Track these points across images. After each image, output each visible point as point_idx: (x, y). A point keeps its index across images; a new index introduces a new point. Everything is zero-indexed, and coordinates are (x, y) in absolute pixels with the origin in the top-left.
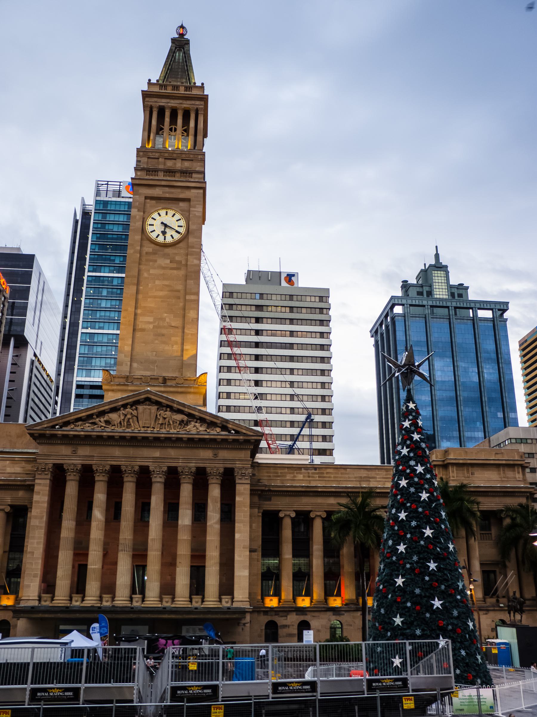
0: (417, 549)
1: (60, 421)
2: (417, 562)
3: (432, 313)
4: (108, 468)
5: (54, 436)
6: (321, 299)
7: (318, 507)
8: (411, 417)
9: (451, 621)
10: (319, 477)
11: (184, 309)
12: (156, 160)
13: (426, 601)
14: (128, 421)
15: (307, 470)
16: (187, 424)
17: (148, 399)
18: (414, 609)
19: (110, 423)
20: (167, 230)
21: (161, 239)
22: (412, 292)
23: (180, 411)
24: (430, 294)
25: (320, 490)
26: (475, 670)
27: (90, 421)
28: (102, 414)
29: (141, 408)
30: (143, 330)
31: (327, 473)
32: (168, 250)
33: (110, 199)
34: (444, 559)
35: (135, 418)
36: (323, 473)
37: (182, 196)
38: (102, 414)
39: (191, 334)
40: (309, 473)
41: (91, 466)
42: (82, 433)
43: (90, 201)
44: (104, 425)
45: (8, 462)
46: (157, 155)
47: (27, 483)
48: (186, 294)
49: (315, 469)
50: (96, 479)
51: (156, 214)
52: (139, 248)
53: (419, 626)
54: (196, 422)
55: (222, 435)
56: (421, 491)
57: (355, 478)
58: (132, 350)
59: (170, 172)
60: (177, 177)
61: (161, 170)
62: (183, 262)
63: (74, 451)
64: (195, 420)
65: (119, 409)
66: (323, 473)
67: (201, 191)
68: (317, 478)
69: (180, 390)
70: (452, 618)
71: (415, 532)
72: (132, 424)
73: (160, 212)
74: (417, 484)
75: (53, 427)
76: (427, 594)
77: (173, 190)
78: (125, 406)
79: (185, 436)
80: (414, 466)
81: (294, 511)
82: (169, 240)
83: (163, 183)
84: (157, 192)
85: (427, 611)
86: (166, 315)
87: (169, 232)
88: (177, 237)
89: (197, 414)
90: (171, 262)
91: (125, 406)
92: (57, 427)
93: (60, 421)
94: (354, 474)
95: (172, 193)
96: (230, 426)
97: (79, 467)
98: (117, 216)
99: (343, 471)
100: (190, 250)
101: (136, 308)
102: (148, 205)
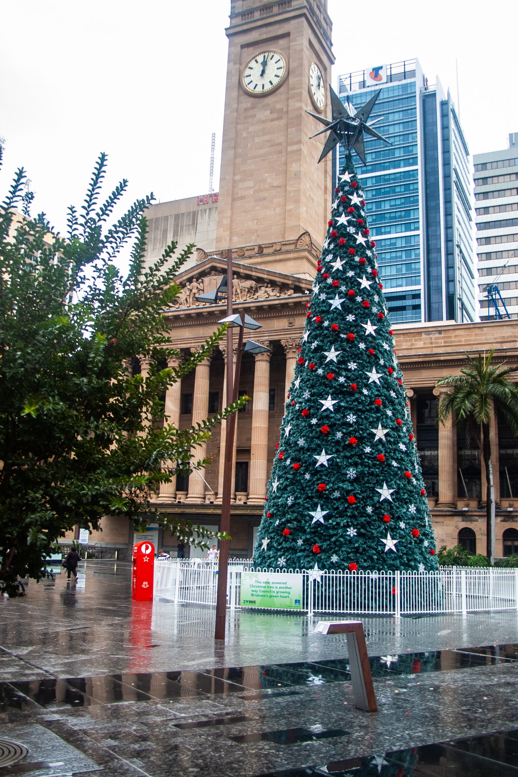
0: (311, 381)
2: (309, 400)
7: (441, 381)
8: (340, 194)
9: (341, 485)
10: (445, 342)
11: (286, 164)
13: (309, 456)
15: (429, 334)
16: (256, 291)
17: (214, 269)
18: (292, 468)
23: (248, 277)
25: (442, 358)
26: (372, 559)
29: (206, 279)
30: (243, 198)
31: (456, 336)
33: (354, 93)
34: (351, 394)
35: (201, 292)
36: (451, 337)
39: (295, 191)
40: (431, 339)
48: (288, 145)
49: (440, 332)
51: (253, 61)
52: (235, 106)
53: (293, 492)
54: (267, 287)
55: (293, 298)
56: (333, 296)
57: (495, 339)
61: (256, 9)
62: (285, 110)
64: (266, 285)
66: (451, 337)
67: (303, 19)
68: (443, 345)
69: (278, 257)
70: (343, 481)
71: (313, 357)
74: (330, 287)
76: (313, 446)
77: (270, 28)
78: (190, 280)
79: (252, 305)
80: (330, 262)
81: (411, 388)
83: (259, 23)
84: (254, 36)
85: (306, 470)
86: (267, 175)
89: (265, 276)
91: (190, 280)
94: (493, 334)
95: (270, 32)
96: (303, 286)
99: (478, 331)
100: (290, 92)
101: (234, 174)
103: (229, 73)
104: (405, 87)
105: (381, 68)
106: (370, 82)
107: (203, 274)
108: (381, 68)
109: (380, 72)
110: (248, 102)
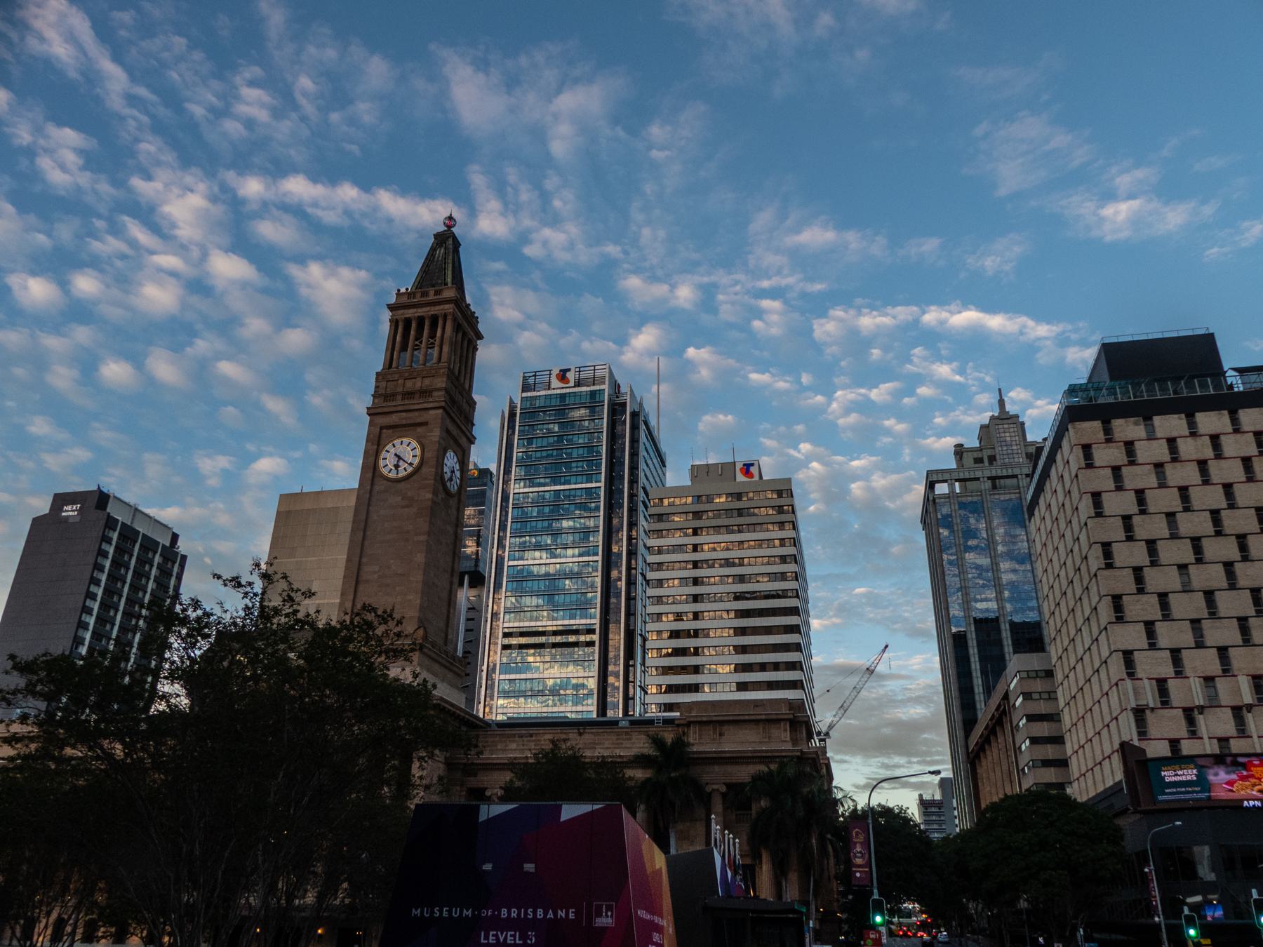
3: (994, 487)
6: (780, 493)
20: (401, 463)
21: (393, 475)
22: (968, 460)
24: (992, 459)
30: (367, 581)
32: (402, 485)
37: (418, 420)
46: (397, 376)
59: (409, 395)
82: (402, 474)
83: (400, 408)
84: (394, 419)
87: (403, 465)
88: (410, 469)
102: (384, 436)
103: (366, 452)
104: (593, 393)
106: (555, 383)
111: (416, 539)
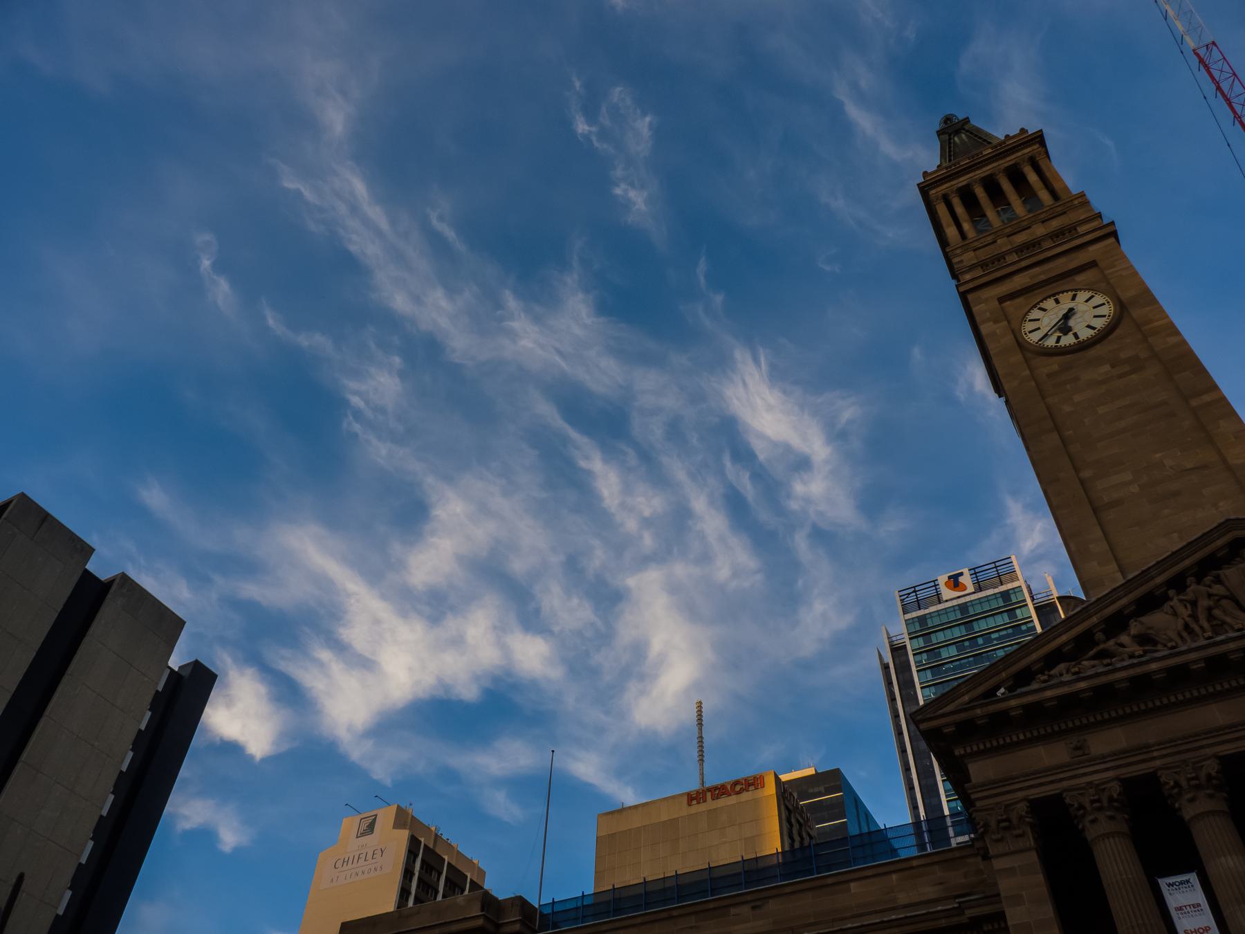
1: (1004, 675)
4: (1212, 767)
5: (1000, 722)
12: (992, 247)
14: (1211, 617)
19: (1155, 643)
21: (1068, 340)
27: (1091, 653)
28: (1116, 624)
29: (1231, 574)
33: (927, 611)
35: (1224, 602)
38: (1116, 624)
41: (1151, 779)
42: (1083, 685)
43: (899, 630)
44: (1138, 650)
45: (894, 876)
46: (990, 239)
47: (969, 913)
50: (1188, 812)
52: (1027, 372)
58: (1112, 549)
60: (1047, 244)
61: (1009, 252)
63: (1077, 748)
65: (1167, 598)
67: (1112, 240)
72: (1228, 619)
73: (1042, 305)
75: (992, 692)
78: (1178, 583)
82: (1085, 334)
83: (1023, 264)
86: (1158, 455)
90: (1113, 366)
92: (1002, 690)
93: (1004, 675)
97: (1115, 789)
98: (948, 632)
101: (1077, 470)
105: (961, 574)
106: (947, 593)
107: (1209, 566)
108: (961, 574)
109: (961, 579)
110: (1054, 364)
111: (1194, 403)
